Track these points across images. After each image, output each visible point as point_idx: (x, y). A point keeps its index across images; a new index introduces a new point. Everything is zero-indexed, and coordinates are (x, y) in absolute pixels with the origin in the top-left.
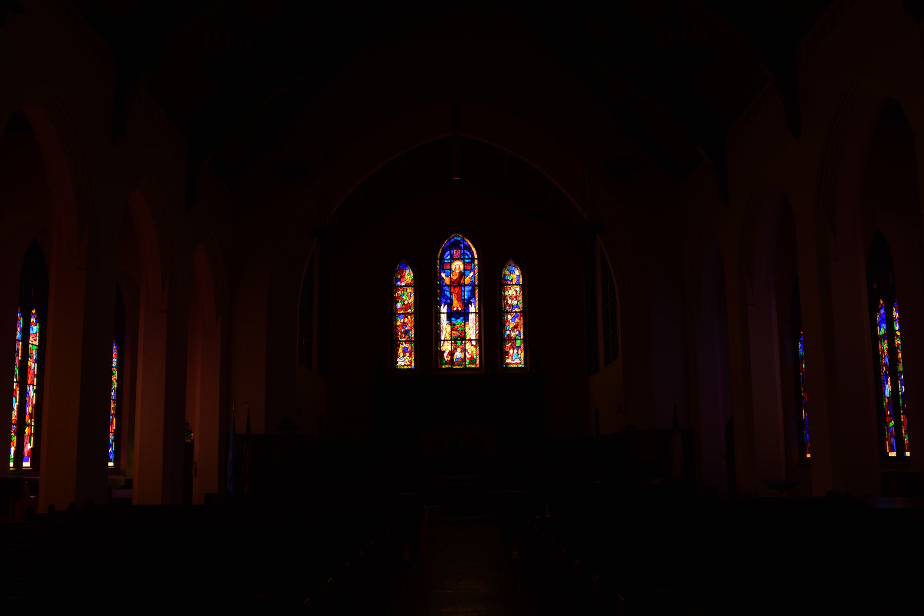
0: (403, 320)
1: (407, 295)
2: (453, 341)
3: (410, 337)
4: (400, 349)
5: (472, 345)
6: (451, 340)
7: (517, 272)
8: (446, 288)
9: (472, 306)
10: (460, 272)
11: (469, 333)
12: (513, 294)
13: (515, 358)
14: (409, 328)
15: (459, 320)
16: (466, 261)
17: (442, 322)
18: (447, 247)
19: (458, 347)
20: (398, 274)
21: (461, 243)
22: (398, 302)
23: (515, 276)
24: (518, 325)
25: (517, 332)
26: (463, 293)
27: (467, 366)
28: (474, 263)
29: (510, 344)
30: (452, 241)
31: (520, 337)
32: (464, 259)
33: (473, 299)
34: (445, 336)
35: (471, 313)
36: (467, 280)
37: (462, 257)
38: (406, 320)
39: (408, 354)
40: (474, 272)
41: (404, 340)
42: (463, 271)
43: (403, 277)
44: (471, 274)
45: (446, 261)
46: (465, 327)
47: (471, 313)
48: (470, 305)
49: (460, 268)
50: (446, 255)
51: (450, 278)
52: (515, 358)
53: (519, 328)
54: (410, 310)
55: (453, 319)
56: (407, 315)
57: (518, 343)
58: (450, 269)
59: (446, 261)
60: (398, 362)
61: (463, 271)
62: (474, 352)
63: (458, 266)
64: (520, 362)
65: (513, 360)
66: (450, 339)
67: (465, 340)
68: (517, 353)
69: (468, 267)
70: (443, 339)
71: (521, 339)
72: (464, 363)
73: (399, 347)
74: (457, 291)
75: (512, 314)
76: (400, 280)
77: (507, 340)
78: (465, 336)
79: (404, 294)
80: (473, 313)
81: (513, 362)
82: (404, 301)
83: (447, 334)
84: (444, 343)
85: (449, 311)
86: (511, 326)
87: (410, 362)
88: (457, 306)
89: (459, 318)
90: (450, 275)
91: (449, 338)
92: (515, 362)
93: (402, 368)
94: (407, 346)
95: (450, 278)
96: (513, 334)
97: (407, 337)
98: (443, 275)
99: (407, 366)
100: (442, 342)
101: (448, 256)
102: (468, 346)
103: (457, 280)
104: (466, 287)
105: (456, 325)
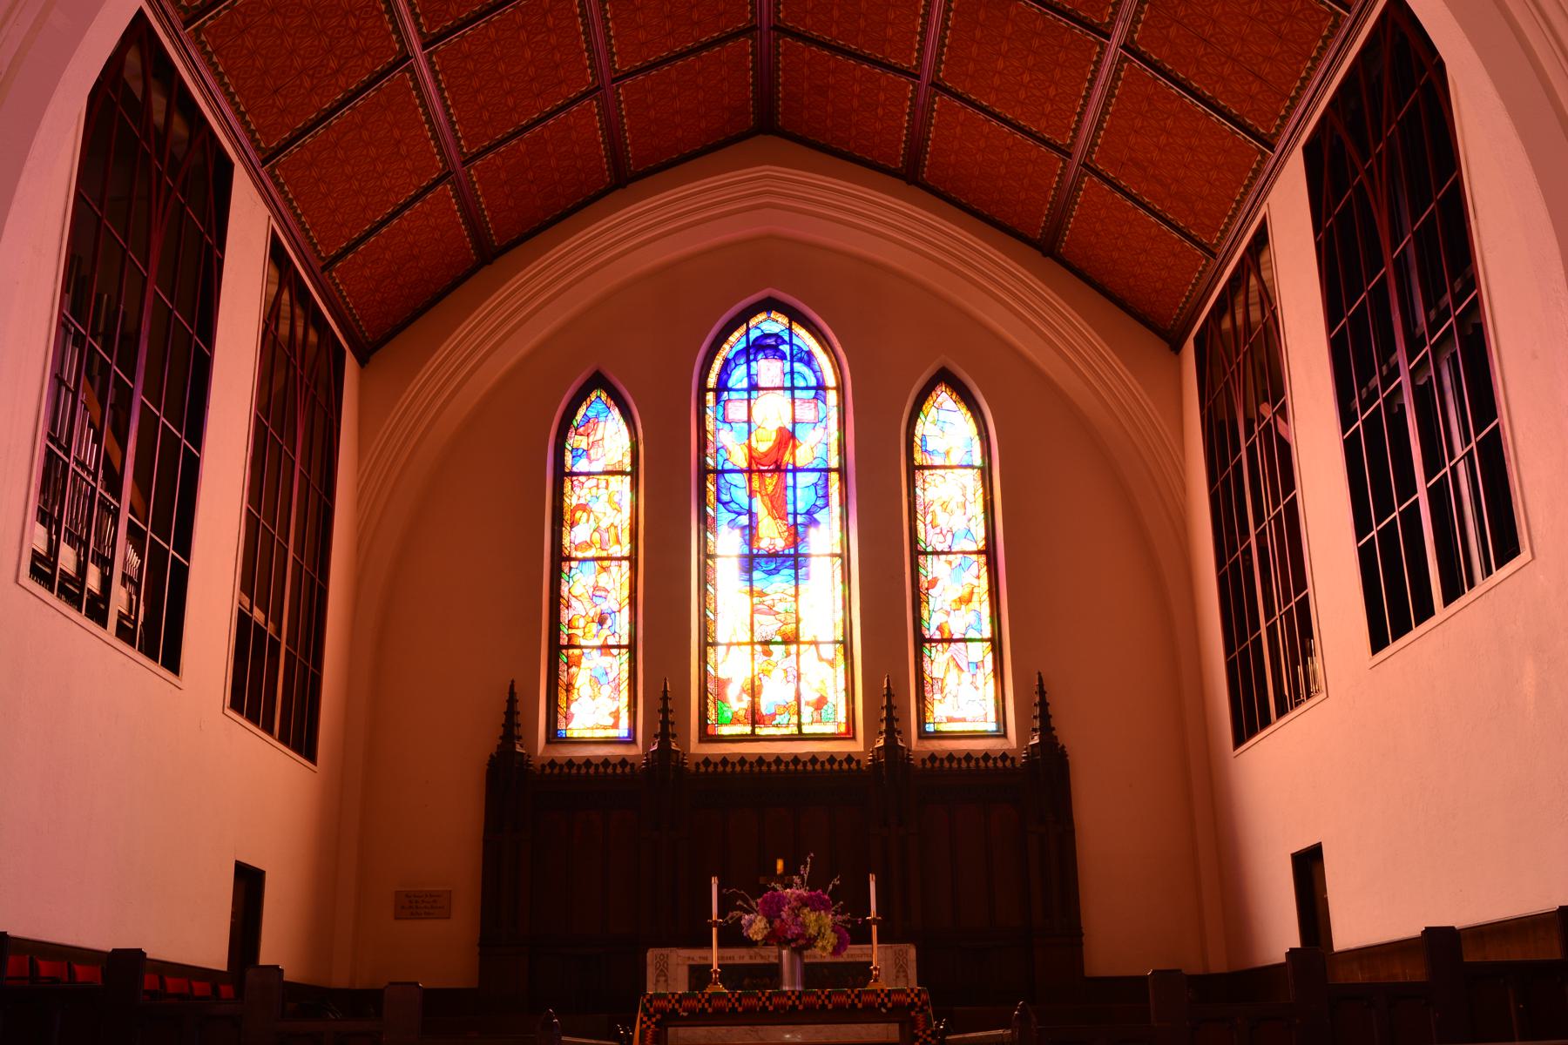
0: (591, 582)
1: (609, 501)
2: (758, 648)
5: (821, 659)
6: (752, 643)
15: (776, 578)
18: (738, 353)
20: (581, 435)
21: (784, 342)
24: (972, 593)
25: (972, 617)
26: (790, 492)
27: (806, 730)
28: (825, 402)
29: (948, 655)
30: (754, 334)
31: (980, 631)
32: (793, 388)
35: (818, 556)
36: (803, 456)
37: (788, 384)
38: (604, 580)
39: (607, 690)
41: (599, 642)
42: (789, 427)
46: (796, 601)
47: (818, 556)
51: (750, 447)
53: (974, 604)
56: (605, 563)
59: (733, 395)
61: (789, 427)
63: (772, 412)
71: (982, 640)
72: (794, 719)
73: (578, 665)
74: (770, 488)
75: (950, 557)
77: (938, 641)
78: (797, 629)
81: (956, 715)
84: (728, 650)
85: (746, 550)
87: (616, 715)
88: (772, 535)
89: (777, 571)
90: (749, 438)
94: (606, 661)
96: (957, 628)
97: (605, 632)
99: (605, 728)
103: (773, 457)
104: (798, 474)
105: (766, 595)
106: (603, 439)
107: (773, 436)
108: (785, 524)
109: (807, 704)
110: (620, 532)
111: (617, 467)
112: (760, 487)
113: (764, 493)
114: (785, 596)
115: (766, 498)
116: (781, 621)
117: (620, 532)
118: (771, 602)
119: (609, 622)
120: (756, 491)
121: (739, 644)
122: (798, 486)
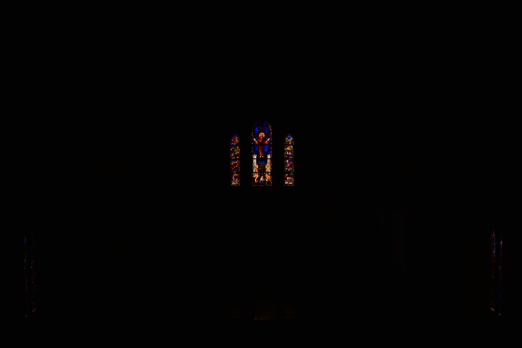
1: (237, 150)
3: (238, 171)
5: (269, 175)
7: (292, 139)
10: (263, 138)
12: (289, 150)
13: (289, 181)
16: (266, 132)
17: (254, 163)
19: (262, 176)
22: (232, 153)
23: (291, 140)
25: (291, 169)
26: (264, 149)
31: (292, 171)
34: (256, 170)
39: (237, 179)
41: (235, 172)
43: (235, 140)
44: (269, 139)
45: (256, 133)
47: (269, 159)
49: (263, 136)
52: (289, 181)
54: (238, 157)
55: (259, 162)
57: (292, 174)
58: (258, 136)
62: (270, 178)
64: (292, 183)
65: (289, 182)
67: (265, 172)
68: (291, 179)
69: (267, 136)
70: (254, 172)
76: (233, 142)
79: (235, 149)
80: (269, 159)
86: (288, 166)
91: (257, 171)
92: (290, 183)
98: (255, 140)
99: (237, 185)
100: (254, 173)
102: (266, 175)
106: (236, 139)
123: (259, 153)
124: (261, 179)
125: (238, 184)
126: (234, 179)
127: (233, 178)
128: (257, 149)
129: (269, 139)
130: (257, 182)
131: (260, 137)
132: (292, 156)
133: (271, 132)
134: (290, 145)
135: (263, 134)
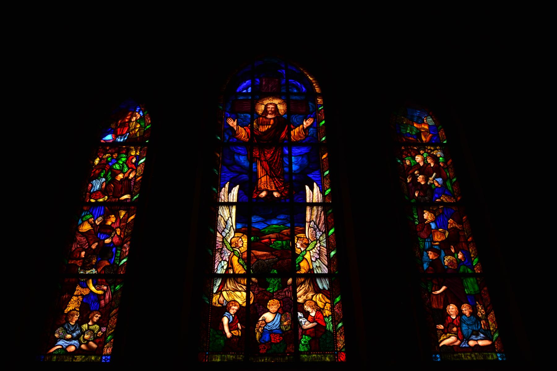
4: (75, 298)
8: (240, 149)
9: (312, 189)
11: (307, 256)
14: (116, 240)
17: (222, 224)
19: (271, 297)
33: (317, 172)
34: (230, 264)
40: (315, 118)
44: (307, 123)
47: (312, 205)
48: (307, 188)
50: (241, 87)
55: (254, 219)
60: (56, 340)
66: (243, 272)
72: (291, 348)
74: (269, 156)
80: (317, 204)
82: (115, 173)
83: (235, 259)
91: (239, 269)
93: (68, 359)
95: (252, 128)
101: (247, 89)
105: (264, 234)
107: (272, 122)
108: (281, 182)
109: (305, 332)
110: (132, 184)
111: (139, 139)
112: (260, 155)
113: (263, 159)
114: (281, 236)
115: (265, 164)
116: (277, 256)
117: (132, 184)
118: (266, 240)
119: (110, 255)
120: (257, 158)
121: (235, 277)
122: (293, 154)
123: (255, 178)
124: (268, 316)
125: (99, 352)
126: (76, 318)
127: (70, 307)
128: (242, 159)
129: (307, 123)
130: (236, 333)
131: (260, 112)
132: (449, 194)
133: (317, 95)
134: (429, 143)
135: (276, 101)
